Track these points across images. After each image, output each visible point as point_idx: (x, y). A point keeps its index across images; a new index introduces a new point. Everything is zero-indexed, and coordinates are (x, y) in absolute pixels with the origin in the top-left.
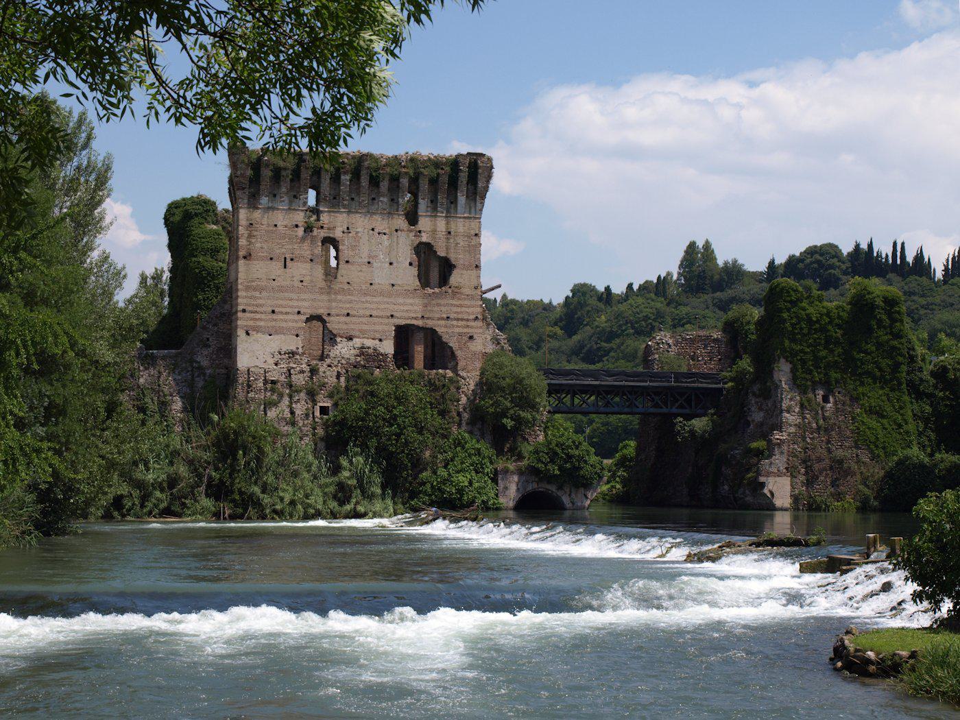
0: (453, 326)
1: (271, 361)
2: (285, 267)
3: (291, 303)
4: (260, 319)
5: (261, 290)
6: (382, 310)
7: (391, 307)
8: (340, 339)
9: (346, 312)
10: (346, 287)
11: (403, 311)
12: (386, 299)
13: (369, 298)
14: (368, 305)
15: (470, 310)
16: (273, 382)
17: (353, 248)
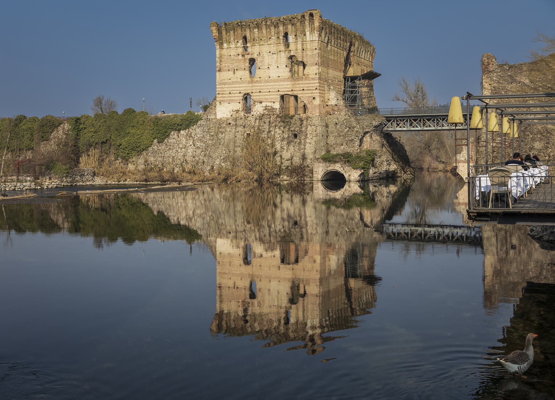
0: (306, 93)
1: (229, 116)
2: (234, 73)
4: (225, 97)
6: (275, 89)
7: (278, 87)
10: (259, 79)
12: (276, 83)
13: (268, 84)
15: (313, 85)
16: (230, 124)
17: (261, 62)
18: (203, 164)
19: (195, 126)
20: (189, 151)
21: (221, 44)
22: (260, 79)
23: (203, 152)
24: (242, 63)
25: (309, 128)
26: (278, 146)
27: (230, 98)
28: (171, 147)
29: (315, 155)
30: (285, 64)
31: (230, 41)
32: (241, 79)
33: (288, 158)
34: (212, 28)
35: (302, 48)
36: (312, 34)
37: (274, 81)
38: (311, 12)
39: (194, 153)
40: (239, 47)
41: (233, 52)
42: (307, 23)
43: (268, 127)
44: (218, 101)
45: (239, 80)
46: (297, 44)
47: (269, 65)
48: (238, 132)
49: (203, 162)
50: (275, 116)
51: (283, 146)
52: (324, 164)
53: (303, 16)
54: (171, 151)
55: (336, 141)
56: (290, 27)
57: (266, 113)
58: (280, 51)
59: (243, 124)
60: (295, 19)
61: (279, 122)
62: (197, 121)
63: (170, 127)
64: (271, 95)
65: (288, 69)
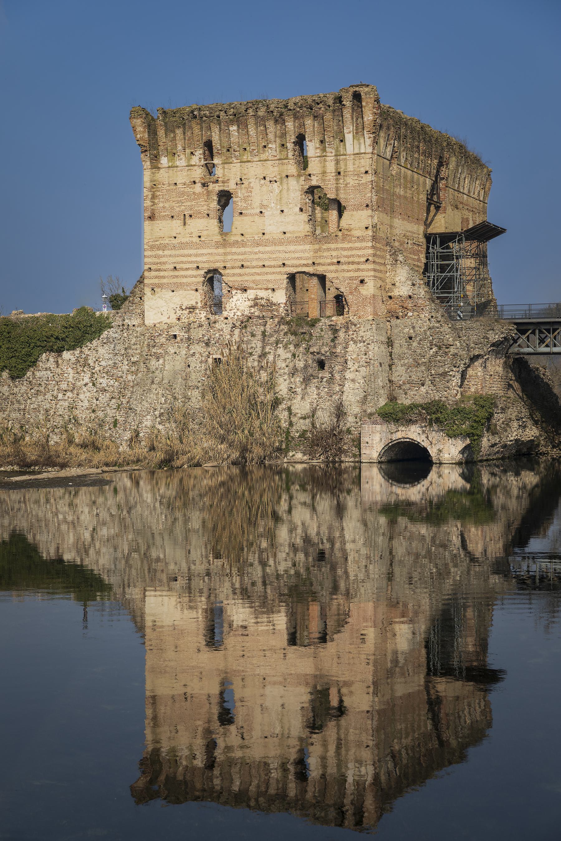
0: (344, 271)
1: (173, 318)
2: (185, 224)
3: (190, 259)
4: (164, 277)
5: (163, 247)
6: (275, 259)
7: (282, 255)
8: (235, 291)
9: (240, 264)
10: (240, 238)
11: (294, 259)
13: (261, 249)
14: (261, 256)
15: (360, 253)
16: (175, 336)
17: (245, 199)
18: (115, 426)
19: (95, 342)
20: (82, 396)
21: (155, 158)
22: (243, 238)
23: (114, 401)
24: (202, 200)
25: (352, 347)
26: (283, 388)
27: (175, 280)
28: (42, 389)
29: (364, 407)
30: (299, 206)
31: (174, 151)
32: (200, 237)
33: (304, 412)
34: (135, 120)
35: (337, 169)
36: (359, 140)
37: (274, 243)
38: (357, 89)
39: (95, 401)
40: (194, 165)
41: (182, 177)
42: (347, 114)
43: (259, 344)
44: (148, 286)
45: (196, 240)
46: (325, 161)
47: (262, 206)
48: (193, 355)
49: (115, 423)
50: (276, 320)
51: (293, 386)
52: (385, 427)
53: (339, 100)
54: (40, 398)
55: (410, 377)
56: (309, 122)
57: (256, 314)
58: (287, 176)
59: (206, 338)
60: (321, 105)
61: (286, 334)
62: (100, 331)
63: (39, 343)
64: (267, 274)
65: (304, 217)
